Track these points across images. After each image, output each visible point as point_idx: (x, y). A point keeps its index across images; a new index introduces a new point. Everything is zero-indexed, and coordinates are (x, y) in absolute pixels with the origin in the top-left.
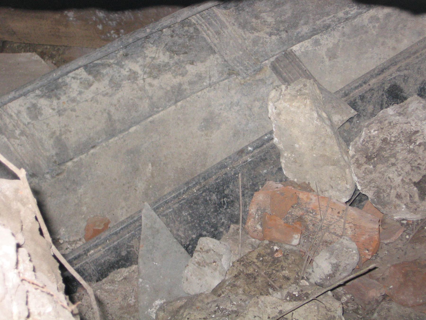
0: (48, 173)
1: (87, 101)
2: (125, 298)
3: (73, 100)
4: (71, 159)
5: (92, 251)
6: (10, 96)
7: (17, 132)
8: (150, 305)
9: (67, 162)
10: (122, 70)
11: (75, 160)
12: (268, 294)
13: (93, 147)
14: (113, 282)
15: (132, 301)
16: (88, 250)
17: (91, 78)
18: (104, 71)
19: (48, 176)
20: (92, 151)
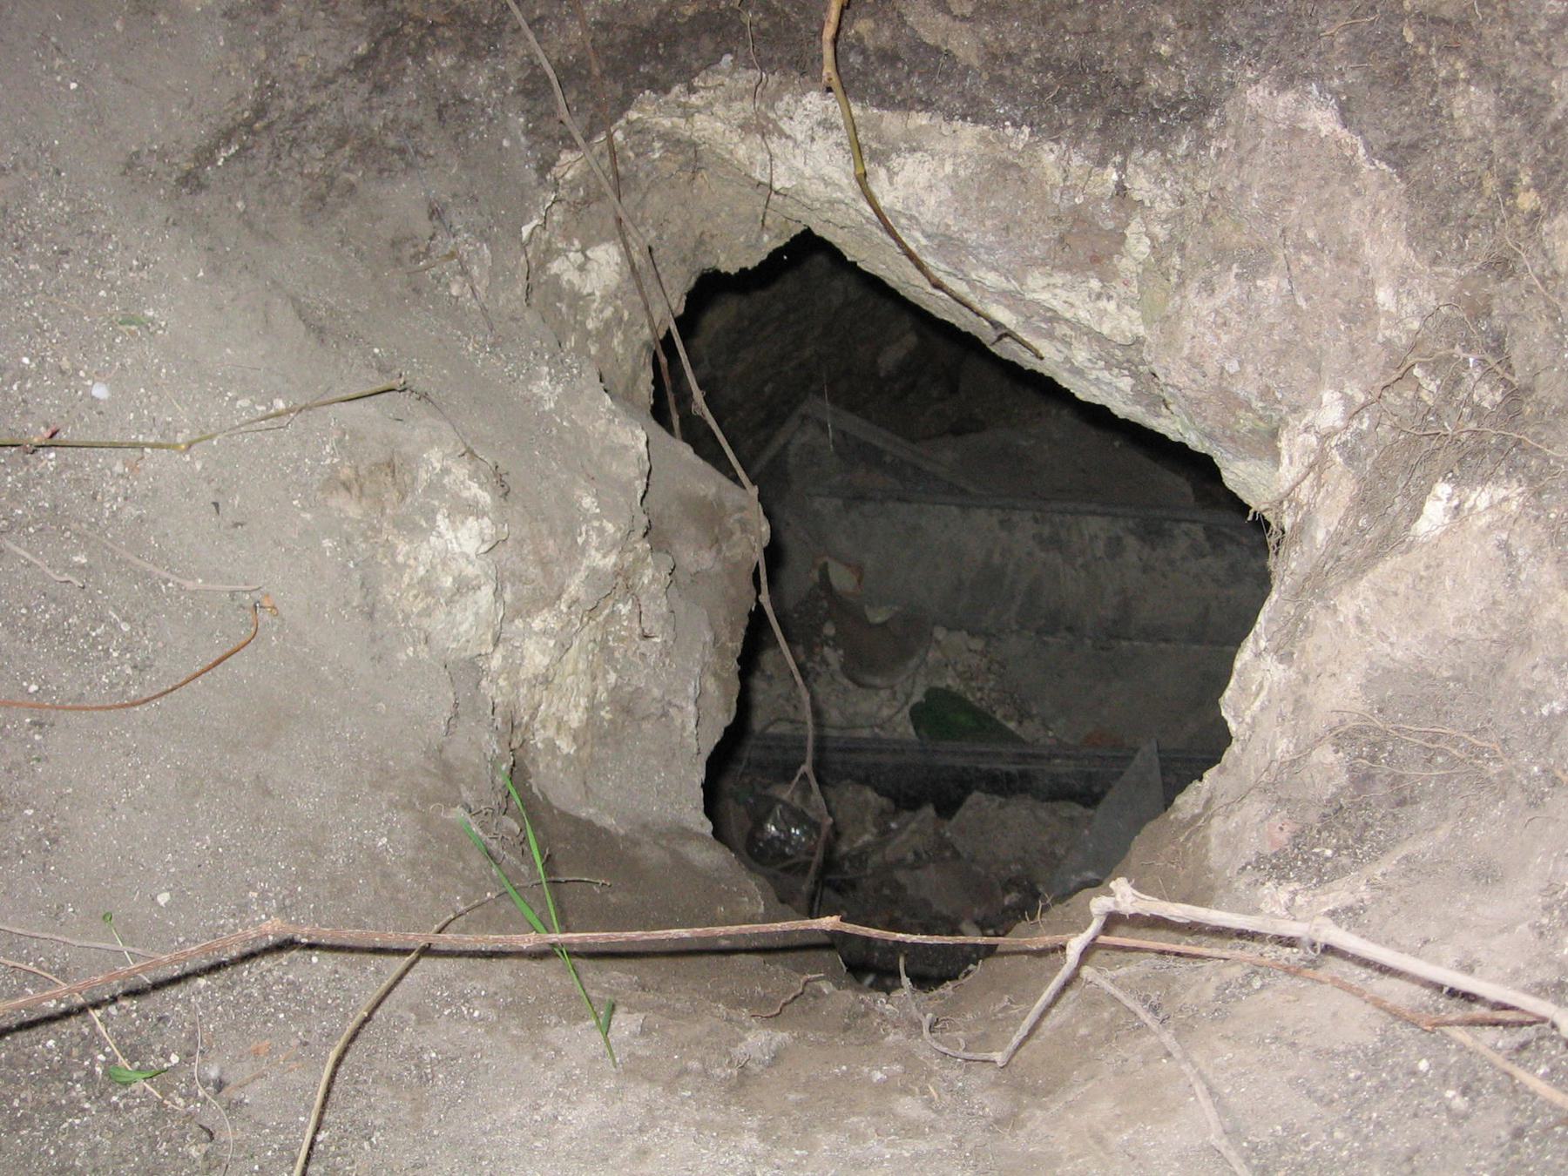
0: (1090, 638)
1: (1187, 573)
2: (1053, 841)
3: (1171, 563)
4: (1130, 639)
5: (1058, 761)
6: (1092, 507)
7: (1080, 561)
8: (1077, 872)
9: (1124, 639)
10: (1252, 560)
11: (1136, 643)
12: (581, 742)
13: (1167, 640)
14: (1054, 813)
15: (1060, 851)
16: (1056, 756)
17: (1207, 546)
18: (1228, 547)
19: (1089, 642)
20: (1163, 645)
